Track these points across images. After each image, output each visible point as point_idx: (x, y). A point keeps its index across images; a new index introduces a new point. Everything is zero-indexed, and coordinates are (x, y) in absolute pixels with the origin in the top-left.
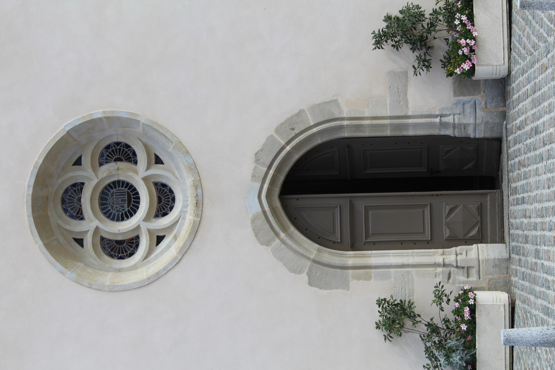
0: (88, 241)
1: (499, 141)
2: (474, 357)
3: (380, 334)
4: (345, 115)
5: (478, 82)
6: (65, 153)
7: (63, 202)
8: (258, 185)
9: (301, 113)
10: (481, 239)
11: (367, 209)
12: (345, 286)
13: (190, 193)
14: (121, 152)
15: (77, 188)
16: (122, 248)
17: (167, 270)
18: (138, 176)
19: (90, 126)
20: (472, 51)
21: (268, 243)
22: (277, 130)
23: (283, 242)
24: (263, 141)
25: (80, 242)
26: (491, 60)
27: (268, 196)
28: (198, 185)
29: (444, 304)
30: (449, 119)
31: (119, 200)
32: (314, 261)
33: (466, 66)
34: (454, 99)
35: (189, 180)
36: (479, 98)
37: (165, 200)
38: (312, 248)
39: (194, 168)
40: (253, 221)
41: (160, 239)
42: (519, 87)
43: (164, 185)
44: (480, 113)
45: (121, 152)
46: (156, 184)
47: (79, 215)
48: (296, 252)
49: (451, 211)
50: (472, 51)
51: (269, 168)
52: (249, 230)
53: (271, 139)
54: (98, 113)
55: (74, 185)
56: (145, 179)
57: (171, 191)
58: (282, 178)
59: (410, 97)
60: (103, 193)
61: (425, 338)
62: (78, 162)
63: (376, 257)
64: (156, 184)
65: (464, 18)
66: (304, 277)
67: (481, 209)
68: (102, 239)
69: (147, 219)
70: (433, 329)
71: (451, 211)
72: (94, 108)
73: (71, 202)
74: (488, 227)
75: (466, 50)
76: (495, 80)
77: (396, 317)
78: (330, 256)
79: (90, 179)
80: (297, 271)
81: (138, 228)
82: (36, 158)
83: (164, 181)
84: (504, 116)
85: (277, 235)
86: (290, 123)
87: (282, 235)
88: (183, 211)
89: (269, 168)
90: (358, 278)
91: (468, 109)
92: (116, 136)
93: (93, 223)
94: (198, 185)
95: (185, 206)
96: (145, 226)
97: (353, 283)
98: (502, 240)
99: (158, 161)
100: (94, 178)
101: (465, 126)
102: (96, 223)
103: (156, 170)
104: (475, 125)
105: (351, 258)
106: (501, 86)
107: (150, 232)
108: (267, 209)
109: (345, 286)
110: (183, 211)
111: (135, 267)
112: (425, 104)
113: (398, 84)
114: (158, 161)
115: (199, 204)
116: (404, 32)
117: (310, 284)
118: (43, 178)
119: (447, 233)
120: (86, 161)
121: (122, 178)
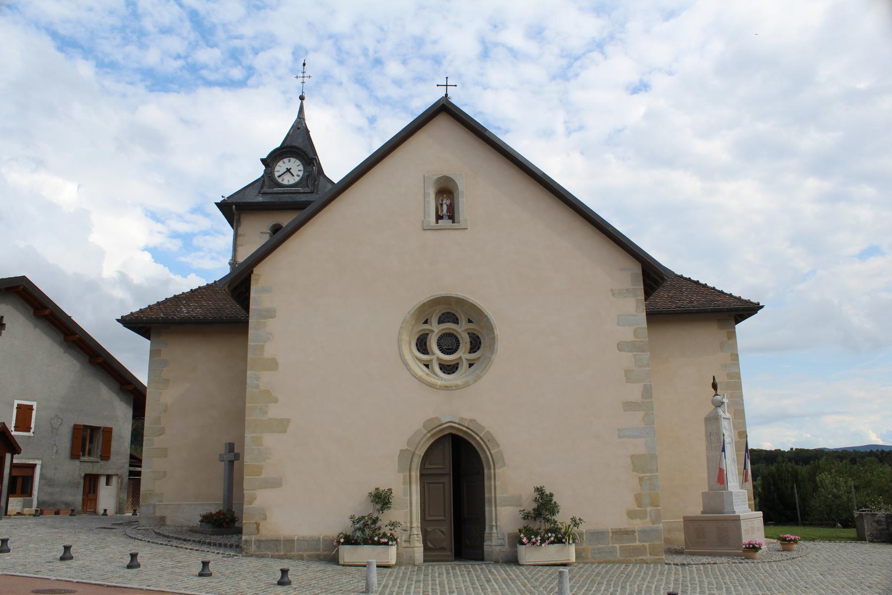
0: (426, 327)
1: (482, 559)
2: (359, 544)
3: (372, 490)
4: (497, 471)
5: (516, 547)
6: (475, 314)
7: (448, 313)
8: (457, 421)
10: (426, 548)
11: (443, 483)
13: (453, 383)
14: (475, 344)
15: (456, 321)
16: (422, 345)
18: (463, 354)
19: (490, 328)
20: (534, 543)
21: (424, 426)
22: (488, 432)
23: (425, 435)
25: (426, 322)
29: (389, 527)
30: (494, 531)
31: (449, 344)
32: (414, 453)
33: (525, 540)
34: (506, 534)
35: (459, 382)
36: (506, 548)
37: (449, 369)
38: (421, 452)
39: (467, 385)
40: (437, 418)
41: (427, 366)
42: (513, 571)
43: (457, 368)
46: (458, 364)
47: (440, 321)
49: (442, 532)
50: (534, 543)
51: (467, 428)
53: (483, 428)
54: (497, 332)
56: (460, 358)
58: (461, 435)
59: (508, 508)
62: (470, 321)
63: (416, 488)
64: (458, 364)
65: (552, 539)
66: (405, 447)
67: (443, 549)
68: (428, 334)
69: (438, 359)
70: (375, 521)
71: (442, 532)
73: (448, 317)
74: (432, 553)
75: (534, 540)
76: (517, 557)
77: (382, 499)
78: (417, 461)
79: (461, 327)
84: (497, 562)
85: (429, 432)
86: (492, 439)
87: (429, 435)
88: (442, 379)
89: (467, 428)
90: (404, 478)
91: (502, 541)
93: (436, 329)
94: (457, 387)
95: (445, 380)
96: (434, 357)
97: (401, 475)
98: (425, 561)
99: (471, 365)
100: (461, 330)
101: (491, 540)
102: (436, 331)
103: (465, 364)
104: (491, 546)
105: (416, 474)
106: (513, 561)
107: (431, 360)
108: (444, 426)
110: (442, 379)
111: (412, 352)
112: (503, 517)
114: (471, 365)
115: (447, 388)
117: (401, 451)
118: (461, 302)
119: (429, 529)
120: (471, 326)
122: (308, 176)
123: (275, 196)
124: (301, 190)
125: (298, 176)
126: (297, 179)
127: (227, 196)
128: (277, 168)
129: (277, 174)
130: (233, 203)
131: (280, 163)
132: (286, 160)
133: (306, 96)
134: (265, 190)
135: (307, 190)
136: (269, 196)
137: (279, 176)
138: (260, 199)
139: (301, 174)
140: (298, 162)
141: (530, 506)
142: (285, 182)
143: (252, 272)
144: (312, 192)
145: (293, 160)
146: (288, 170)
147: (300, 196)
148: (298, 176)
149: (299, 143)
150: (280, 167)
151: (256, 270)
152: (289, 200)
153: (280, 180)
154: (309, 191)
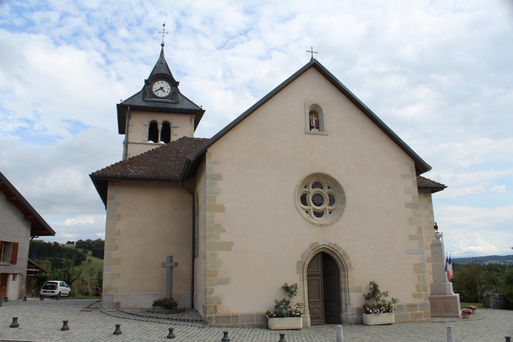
0: (306, 189)
1: (339, 322)
2: (284, 317)
3: (283, 284)
4: (349, 273)
5: (362, 315)
6: (333, 183)
7: (317, 182)
8: (327, 244)
9: (349, 258)
10: (311, 318)
11: (318, 280)
12: (298, 273)
13: (321, 223)
14: (332, 201)
15: (322, 188)
16: (304, 200)
17: (301, 214)
18: (325, 206)
19: (342, 192)
20: (375, 313)
21: (310, 247)
22: (343, 251)
23: (310, 252)
24: (340, 246)
25: (305, 187)
26: (372, 319)
27: (324, 248)
28: (327, 225)
29: (296, 306)
30: (348, 307)
31: (318, 200)
32: (305, 263)
33: (371, 311)
34: (354, 308)
35: (327, 222)
36: (355, 316)
37: (319, 214)
38: (308, 262)
39: (331, 224)
40: (317, 243)
41: (307, 212)
42: (363, 328)
43: (323, 214)
44: (351, 316)
45: (332, 201)
46: (323, 212)
47: (313, 187)
48: (307, 257)
49: (318, 308)
50: (375, 313)
51: (332, 248)
52: (314, 241)
53: (341, 248)
54: (346, 194)
55: (322, 186)
56: (325, 208)
57: (321, 216)
58: (328, 252)
59: (355, 293)
60: (320, 195)
61: (284, 301)
62: (329, 188)
63: (306, 283)
64: (323, 212)
65: (384, 310)
66: (300, 259)
67: (319, 318)
68: (306, 194)
69: (314, 208)
70: (288, 303)
71: (318, 308)
72: (348, 194)
73: (317, 185)
74: (315, 321)
75: (376, 311)
76: (362, 321)
77: (289, 290)
78: (306, 267)
79: (324, 191)
80: (302, 257)
81: (311, 205)
82: (333, 175)
83: (324, 214)
84: (351, 324)
85: (312, 251)
86: (346, 255)
87: (313, 252)
88: (316, 220)
89: (332, 248)
90: (300, 277)
91: (352, 312)
92: (338, 200)
93: (312, 191)
94: (327, 225)
95: (318, 221)
96: (311, 208)
97: (298, 275)
98: (311, 325)
99: (330, 213)
100: (325, 192)
101: (347, 312)
102: (312, 192)
103: (328, 212)
104: (347, 315)
105: (305, 274)
106: (361, 323)
107: (310, 209)
108: (320, 247)
109: (298, 273)
110: (316, 220)
111: (299, 204)
112: (353, 299)
113: (358, 290)
114: (330, 213)
115: (321, 225)
116: (374, 291)
117: (298, 261)
118: (326, 177)
119: (311, 307)
120: (330, 190)
121: (325, 201)
122: (174, 93)
123: (153, 103)
124: (169, 100)
125: (167, 92)
126: (167, 94)
127: (123, 100)
128: (154, 86)
129: (154, 90)
130: (128, 106)
131: (156, 83)
132: (160, 82)
133: (165, 44)
134: (147, 99)
135: (173, 101)
136: (150, 103)
137: (156, 91)
138: (144, 104)
139: (169, 91)
140: (167, 84)
141: (366, 291)
142: (159, 95)
143: (206, 151)
144: (176, 103)
145: (164, 82)
146: (162, 88)
147: (170, 104)
148: (167, 92)
149: (163, 71)
150: (157, 86)
151: (209, 150)
152: (164, 107)
153: (156, 94)
154: (174, 102)
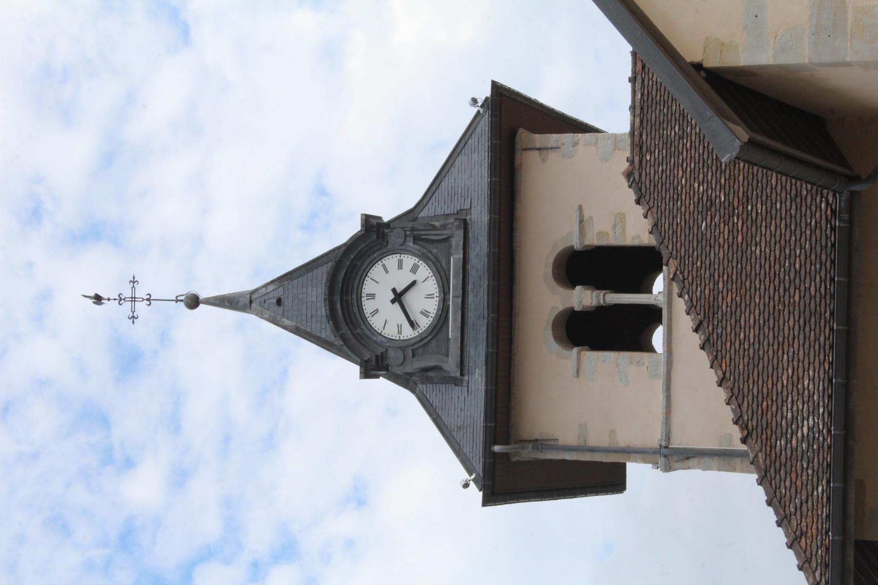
122: (416, 239)
123: (470, 333)
124: (456, 258)
125: (414, 269)
126: (425, 271)
127: (464, 475)
128: (391, 332)
129: (408, 333)
130: (488, 453)
131: (376, 323)
132: (368, 306)
133: (184, 290)
134: (451, 365)
135: (457, 240)
136: (471, 351)
137: (412, 324)
138: (478, 378)
139: (409, 261)
140: (376, 271)
142: (433, 306)
143: (698, 67)
144: (465, 225)
145: (368, 287)
146: (398, 297)
147: (472, 254)
148: (414, 269)
149: (316, 293)
150: (386, 320)
151: (692, 53)
152: (485, 283)
153: (424, 323)
154: (460, 233)
